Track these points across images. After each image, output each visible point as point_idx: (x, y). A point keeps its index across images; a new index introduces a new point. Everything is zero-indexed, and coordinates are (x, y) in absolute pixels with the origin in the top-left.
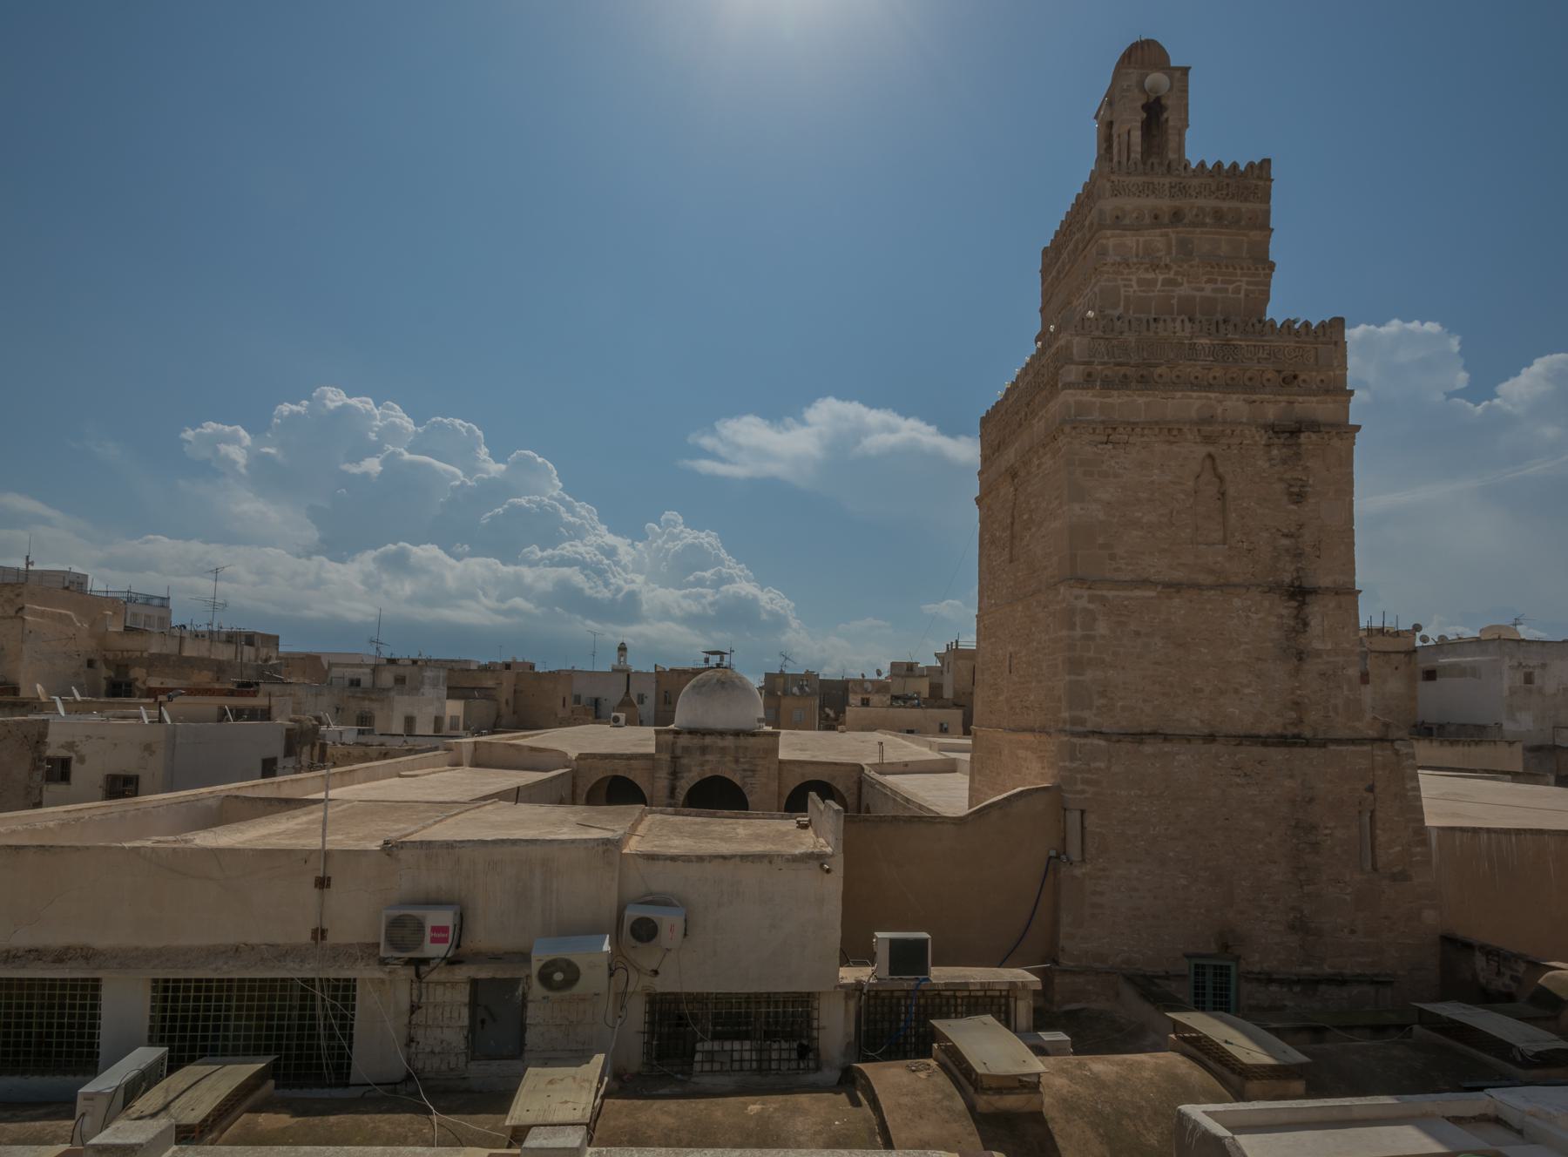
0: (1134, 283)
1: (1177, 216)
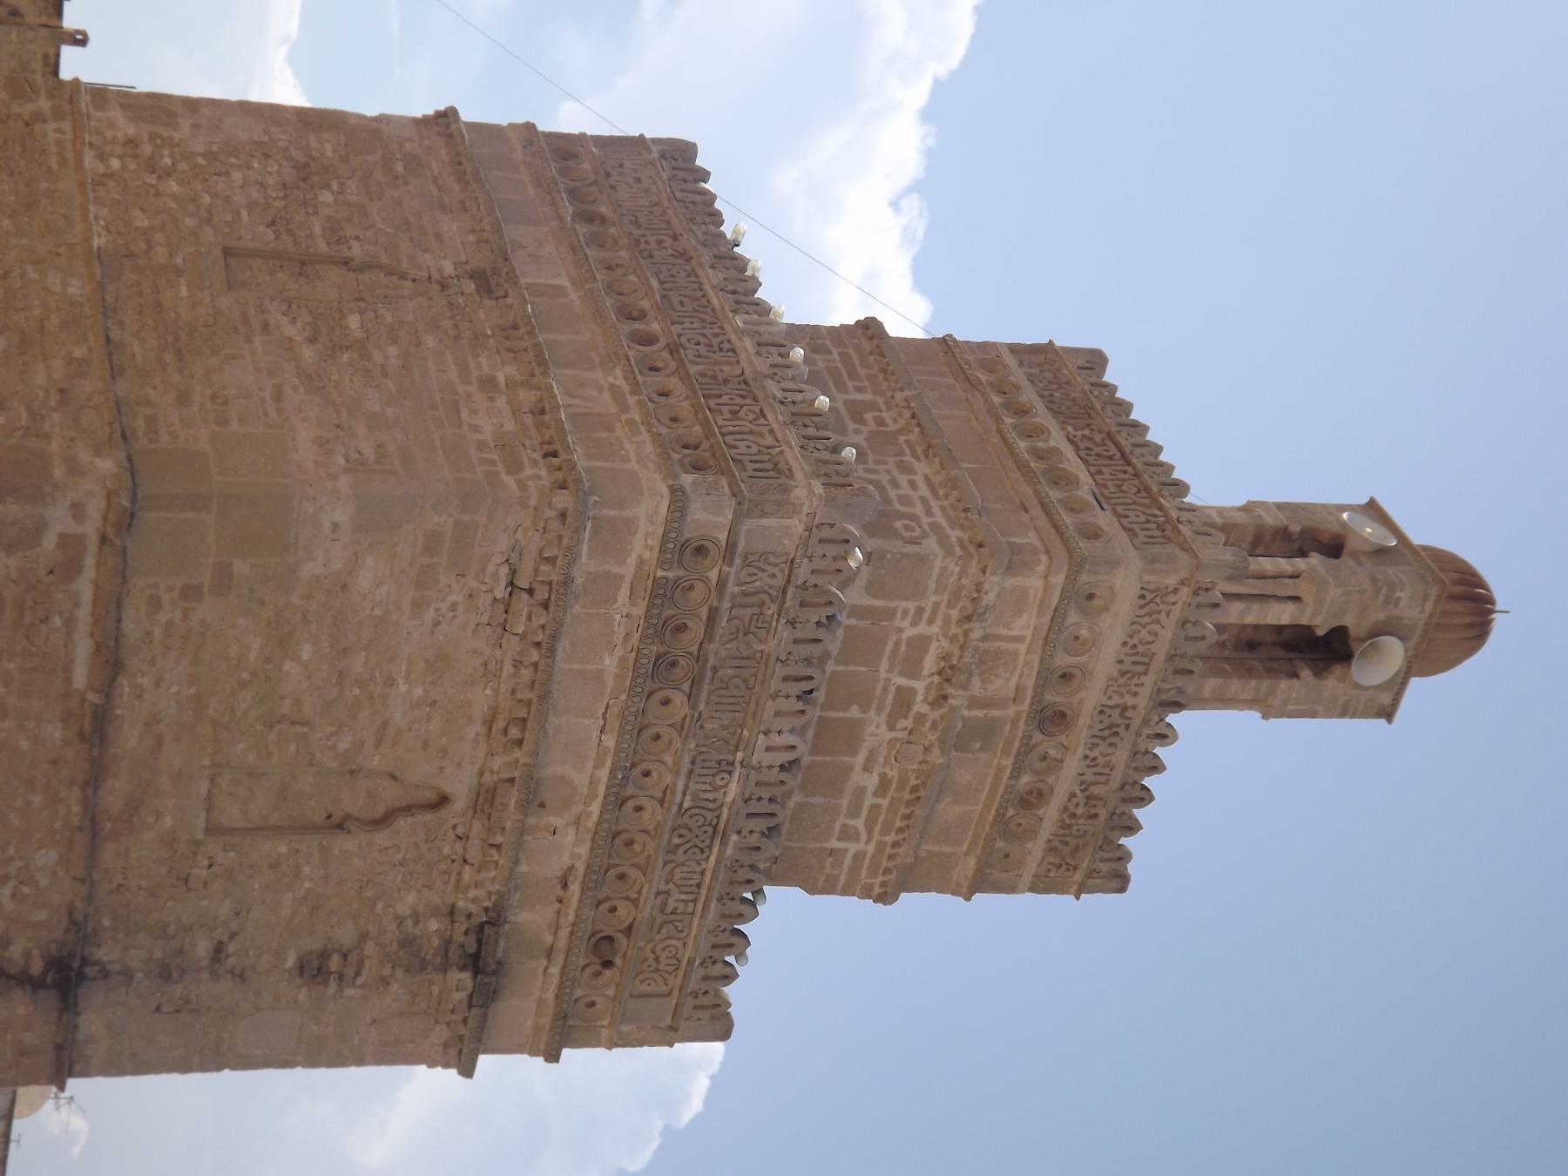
0: (922, 629)
1: (1053, 719)
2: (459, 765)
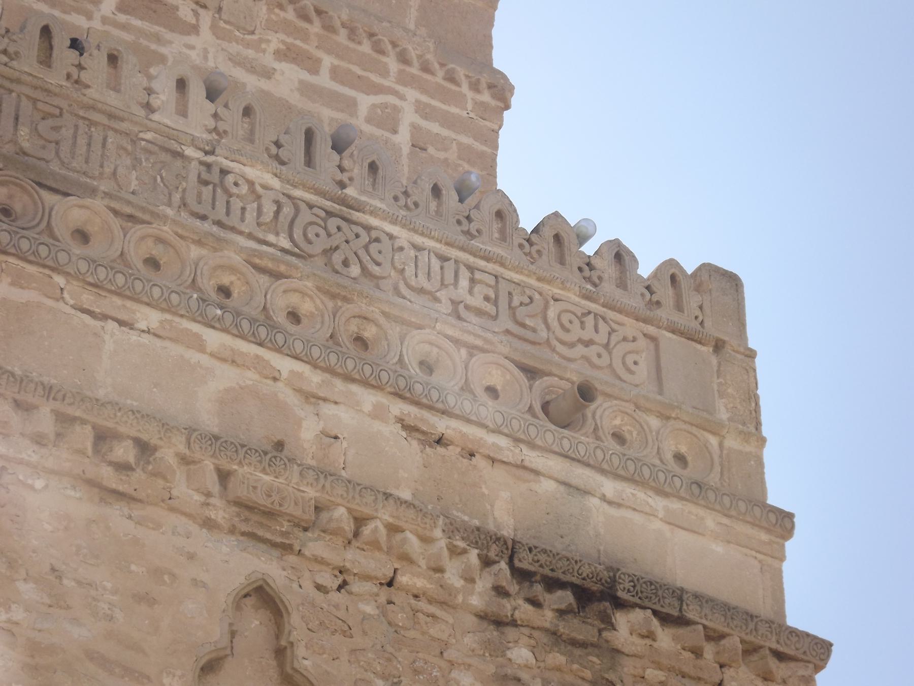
2: (191, 557)
